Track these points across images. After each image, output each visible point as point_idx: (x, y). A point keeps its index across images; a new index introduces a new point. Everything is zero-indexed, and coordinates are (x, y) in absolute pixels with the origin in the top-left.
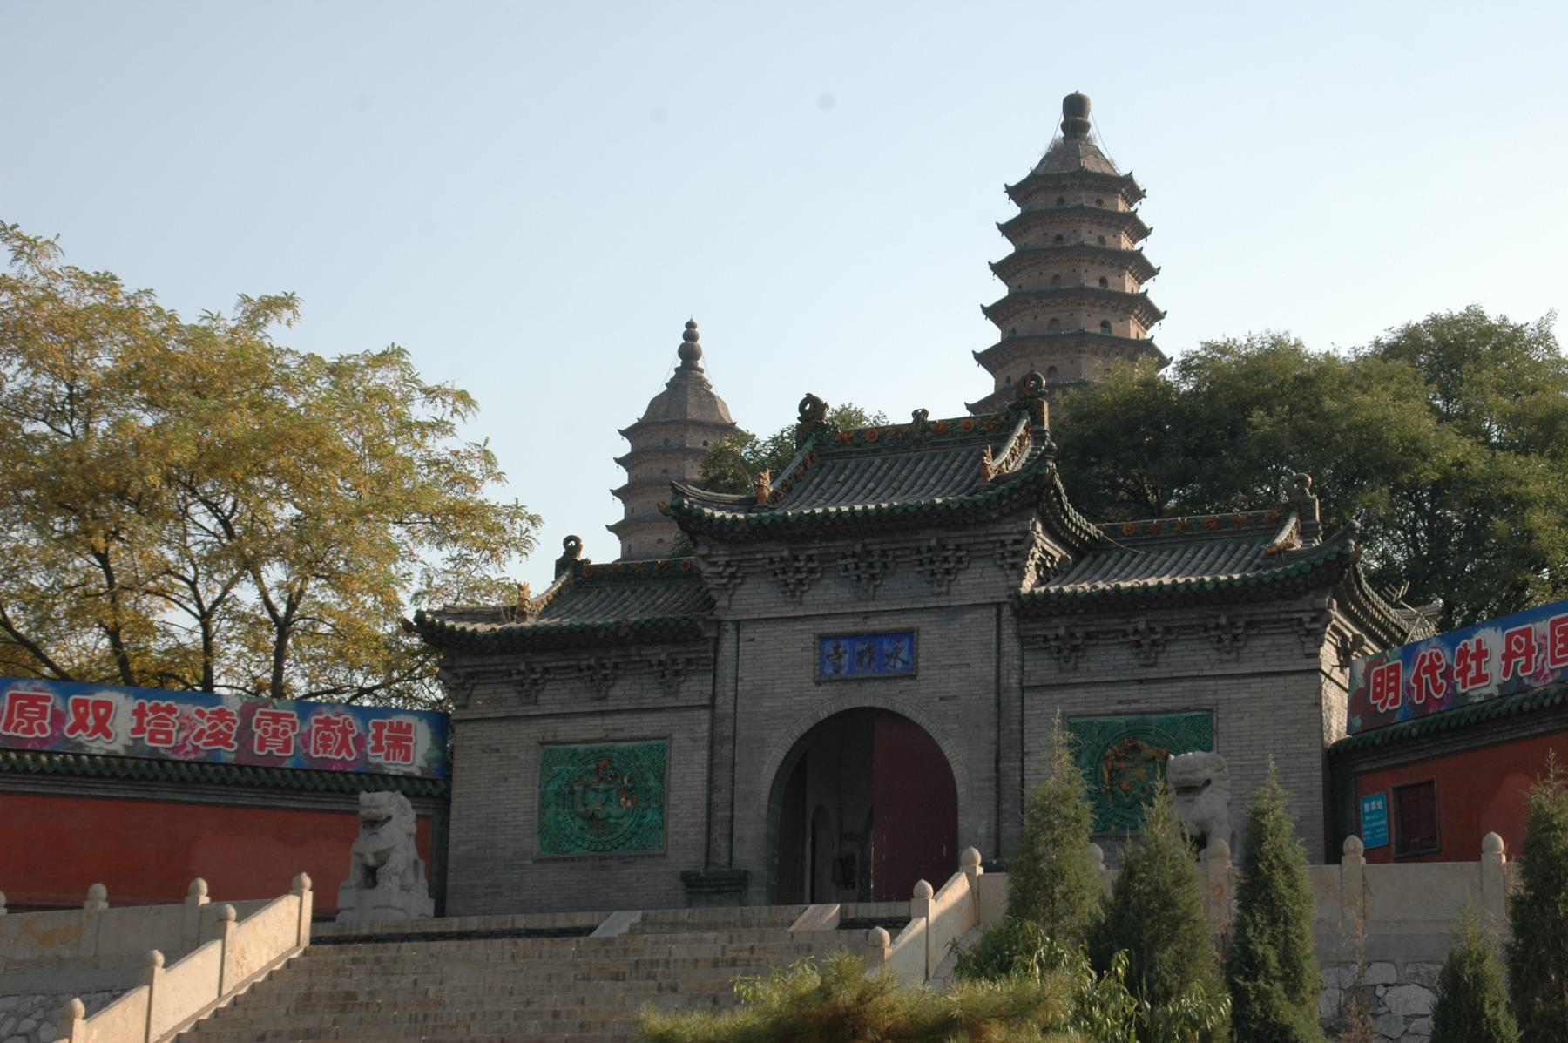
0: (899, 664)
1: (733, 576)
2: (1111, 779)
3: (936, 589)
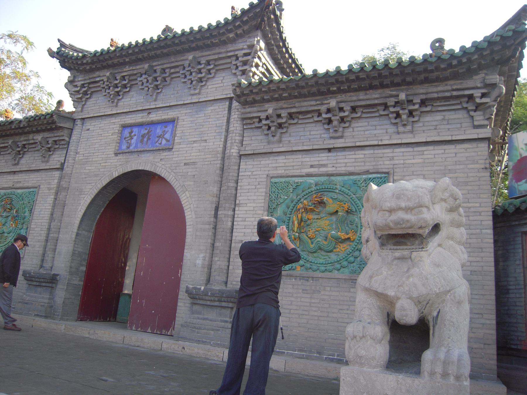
0: (164, 142)
1: (85, 93)
2: (299, 227)
3: (192, 92)
